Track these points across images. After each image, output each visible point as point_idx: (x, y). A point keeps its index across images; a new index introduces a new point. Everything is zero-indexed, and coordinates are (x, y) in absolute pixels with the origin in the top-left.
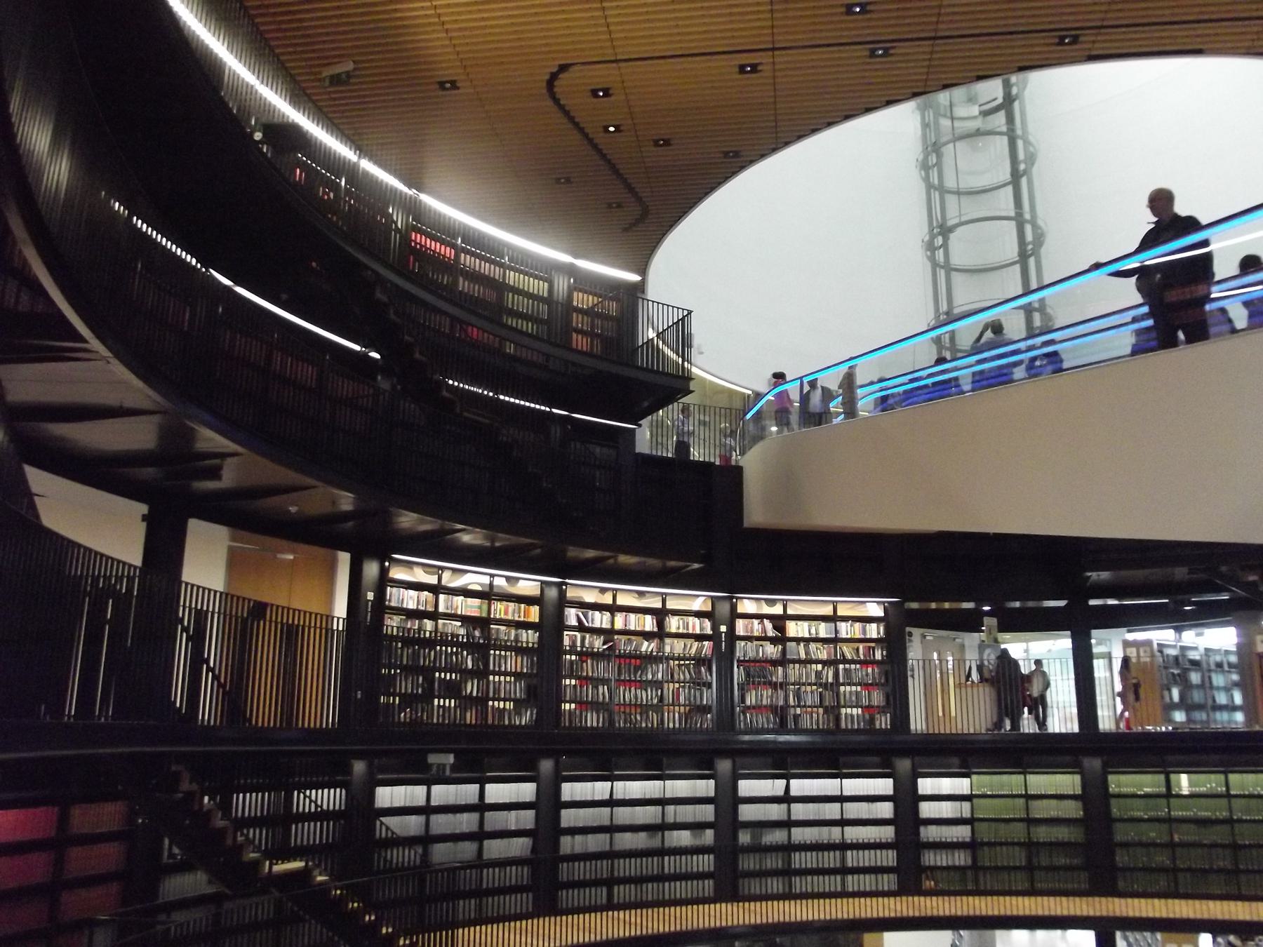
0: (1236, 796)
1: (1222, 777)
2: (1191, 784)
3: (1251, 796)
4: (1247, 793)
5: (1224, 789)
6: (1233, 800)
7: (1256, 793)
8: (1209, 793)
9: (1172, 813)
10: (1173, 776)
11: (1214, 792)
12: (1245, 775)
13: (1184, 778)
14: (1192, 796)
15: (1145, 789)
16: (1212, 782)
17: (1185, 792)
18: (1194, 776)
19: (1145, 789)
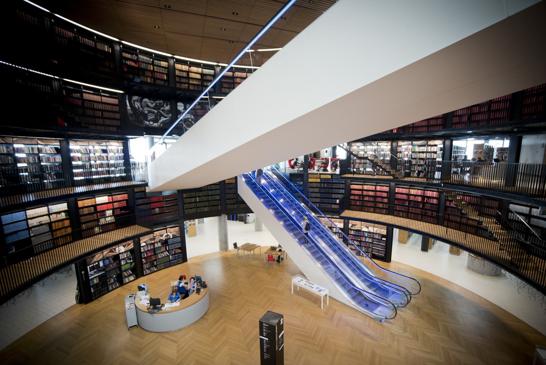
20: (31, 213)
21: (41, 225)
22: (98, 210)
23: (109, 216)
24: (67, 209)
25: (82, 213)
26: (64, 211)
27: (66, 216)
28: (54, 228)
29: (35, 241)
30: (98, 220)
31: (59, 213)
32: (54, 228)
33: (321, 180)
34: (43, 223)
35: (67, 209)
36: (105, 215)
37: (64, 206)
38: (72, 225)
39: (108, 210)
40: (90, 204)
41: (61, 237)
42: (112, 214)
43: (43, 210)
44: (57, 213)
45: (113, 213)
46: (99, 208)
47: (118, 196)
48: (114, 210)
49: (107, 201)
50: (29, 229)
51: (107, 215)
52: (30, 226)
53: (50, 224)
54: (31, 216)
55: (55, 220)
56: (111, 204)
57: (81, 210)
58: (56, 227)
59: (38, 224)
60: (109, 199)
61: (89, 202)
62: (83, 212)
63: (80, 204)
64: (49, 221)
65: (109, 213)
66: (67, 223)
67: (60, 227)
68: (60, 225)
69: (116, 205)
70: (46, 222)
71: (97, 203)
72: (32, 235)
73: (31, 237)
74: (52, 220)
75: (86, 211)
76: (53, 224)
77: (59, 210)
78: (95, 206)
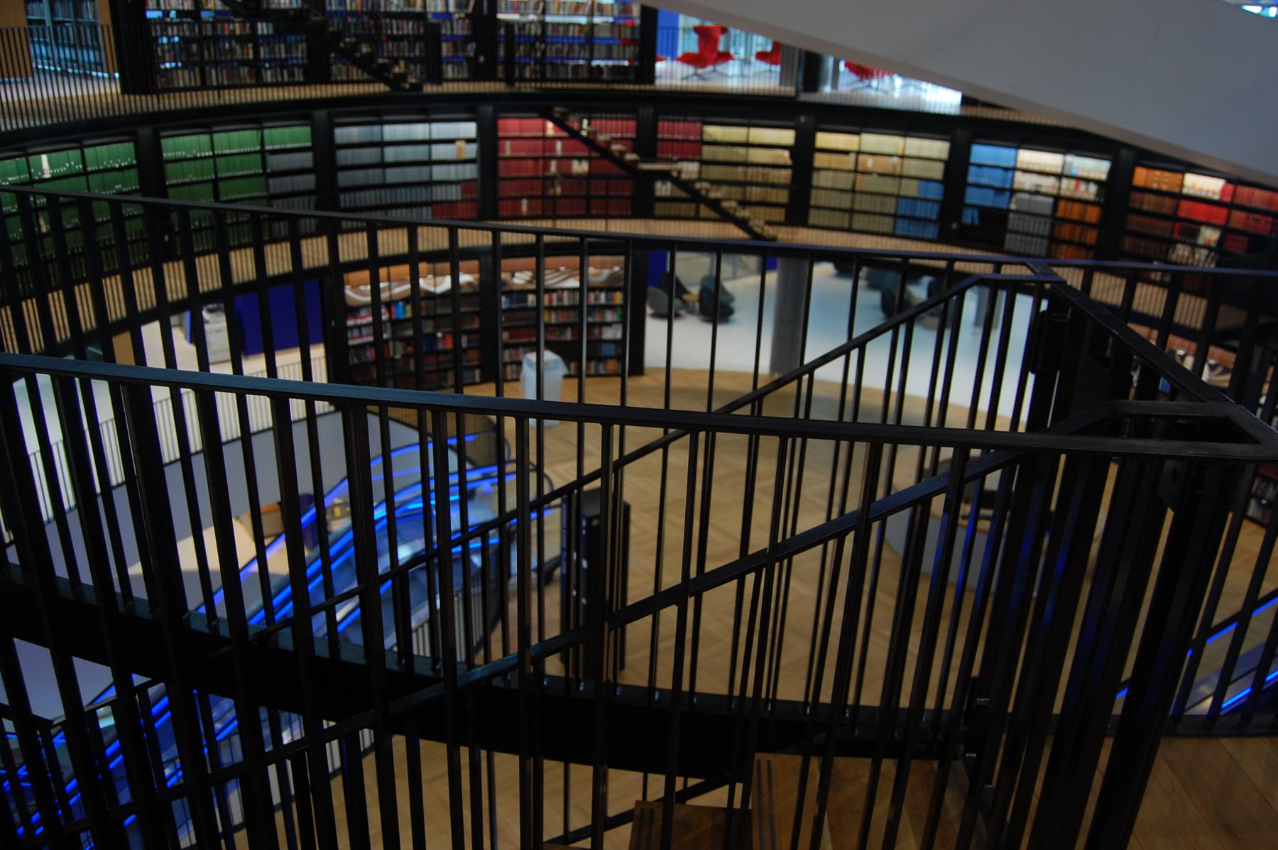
0: (93, 172)
1: (77, 153)
2: (52, 166)
3: (106, 170)
4: (101, 168)
5: (81, 166)
6: (91, 177)
7: (109, 166)
8: (69, 172)
9: (38, 202)
10: (32, 159)
11: (73, 171)
12: (97, 148)
13: (44, 158)
14: (54, 178)
15: (10, 179)
16: (70, 160)
17: (47, 176)
18: (53, 155)
19: (10, 179)
20: (1027, 157)
21: (1037, 193)
22: (1182, 214)
23: (1204, 247)
24: (1103, 177)
25: (1137, 205)
26: (1097, 182)
27: (1098, 194)
28: (1060, 214)
29: (1013, 220)
30: (1172, 243)
31: (1087, 180)
32: (1060, 214)
33: (700, 152)
34: (1044, 190)
35: (1103, 177)
36: (1195, 234)
37: (1098, 168)
38: (1100, 226)
39: (1209, 225)
40: (1164, 188)
41: (1070, 243)
42: (1213, 245)
43: (1050, 160)
44: (1079, 179)
45: (1221, 241)
46: (1185, 209)
47: (1258, 193)
48: (1226, 231)
49: (1216, 197)
50: (1013, 191)
51: (1201, 241)
52: (1016, 186)
53: (1057, 198)
54: (1025, 166)
55: (1068, 194)
56: (1224, 211)
57: (1136, 196)
58: (1065, 211)
59: (1033, 188)
60: (1223, 190)
61: (1166, 180)
62: (1142, 202)
63: (1142, 176)
64: (1055, 192)
65: (1209, 235)
66: (1093, 214)
67: (1075, 216)
68: (1075, 212)
69: (1238, 218)
70: (1050, 191)
71: (1185, 191)
72: (1013, 206)
73: (1009, 211)
74: (1063, 193)
75: (1149, 203)
76: (1062, 204)
77: (1085, 174)
78: (1179, 196)
